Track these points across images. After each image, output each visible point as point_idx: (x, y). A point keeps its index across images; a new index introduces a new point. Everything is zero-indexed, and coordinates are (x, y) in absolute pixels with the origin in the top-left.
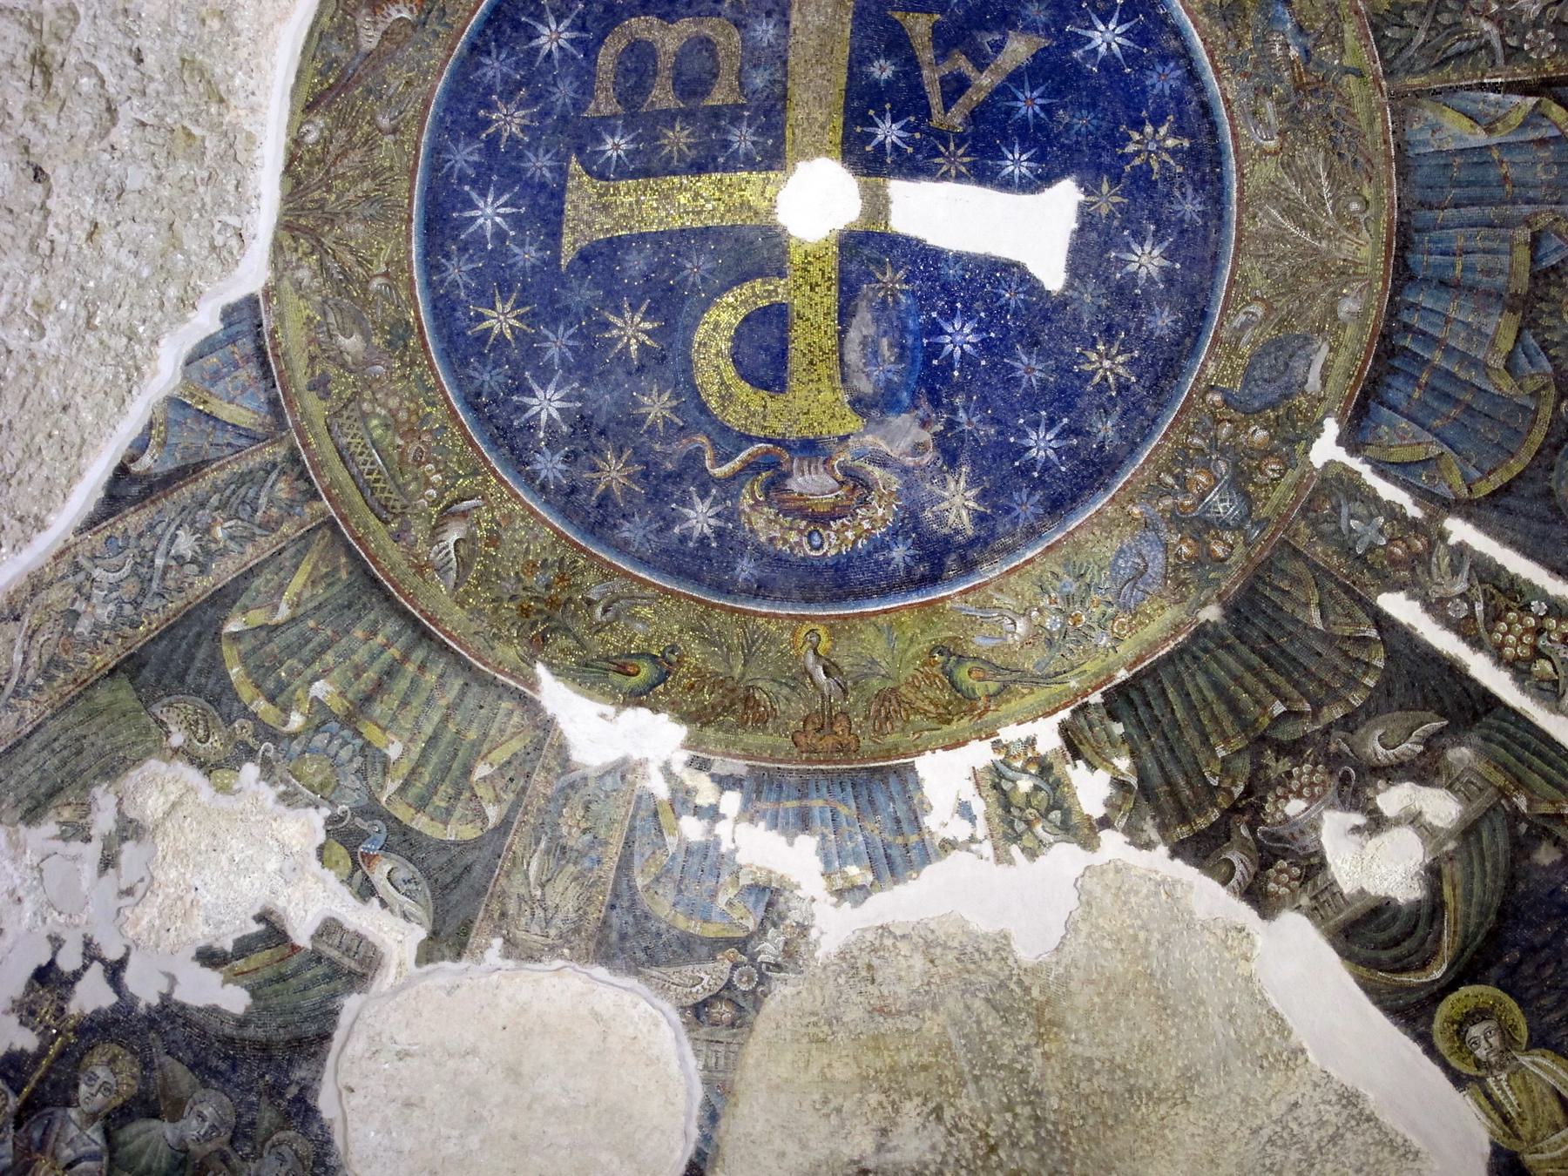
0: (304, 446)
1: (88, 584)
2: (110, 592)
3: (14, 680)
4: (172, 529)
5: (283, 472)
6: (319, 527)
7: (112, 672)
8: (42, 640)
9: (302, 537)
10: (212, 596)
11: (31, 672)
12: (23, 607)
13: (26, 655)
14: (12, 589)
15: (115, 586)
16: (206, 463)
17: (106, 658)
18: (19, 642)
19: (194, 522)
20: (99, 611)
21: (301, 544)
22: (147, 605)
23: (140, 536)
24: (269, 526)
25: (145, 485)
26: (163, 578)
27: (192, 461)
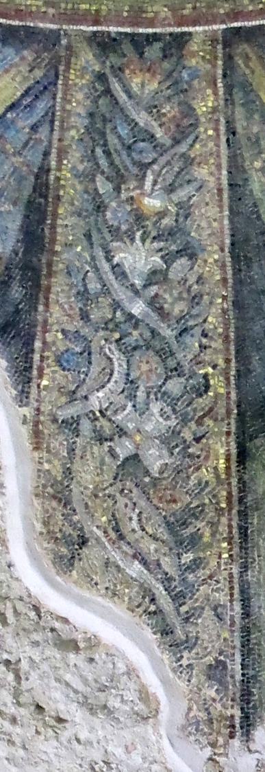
0: (96, 22)
1: (103, 422)
2: (132, 397)
3: (159, 590)
4: (106, 266)
5: (118, 71)
6: (229, 59)
7: (243, 456)
8: (135, 524)
9: (229, 89)
10: (235, 257)
11: (168, 564)
12: (73, 525)
13: (139, 556)
14: (39, 527)
15: (131, 382)
16: (44, 170)
17: (221, 449)
18: (116, 557)
19: (115, 232)
20: (149, 427)
21: (238, 96)
22: (184, 357)
23: (85, 316)
24: (185, 128)
25: (16, 273)
26: (161, 311)
27: (27, 192)
